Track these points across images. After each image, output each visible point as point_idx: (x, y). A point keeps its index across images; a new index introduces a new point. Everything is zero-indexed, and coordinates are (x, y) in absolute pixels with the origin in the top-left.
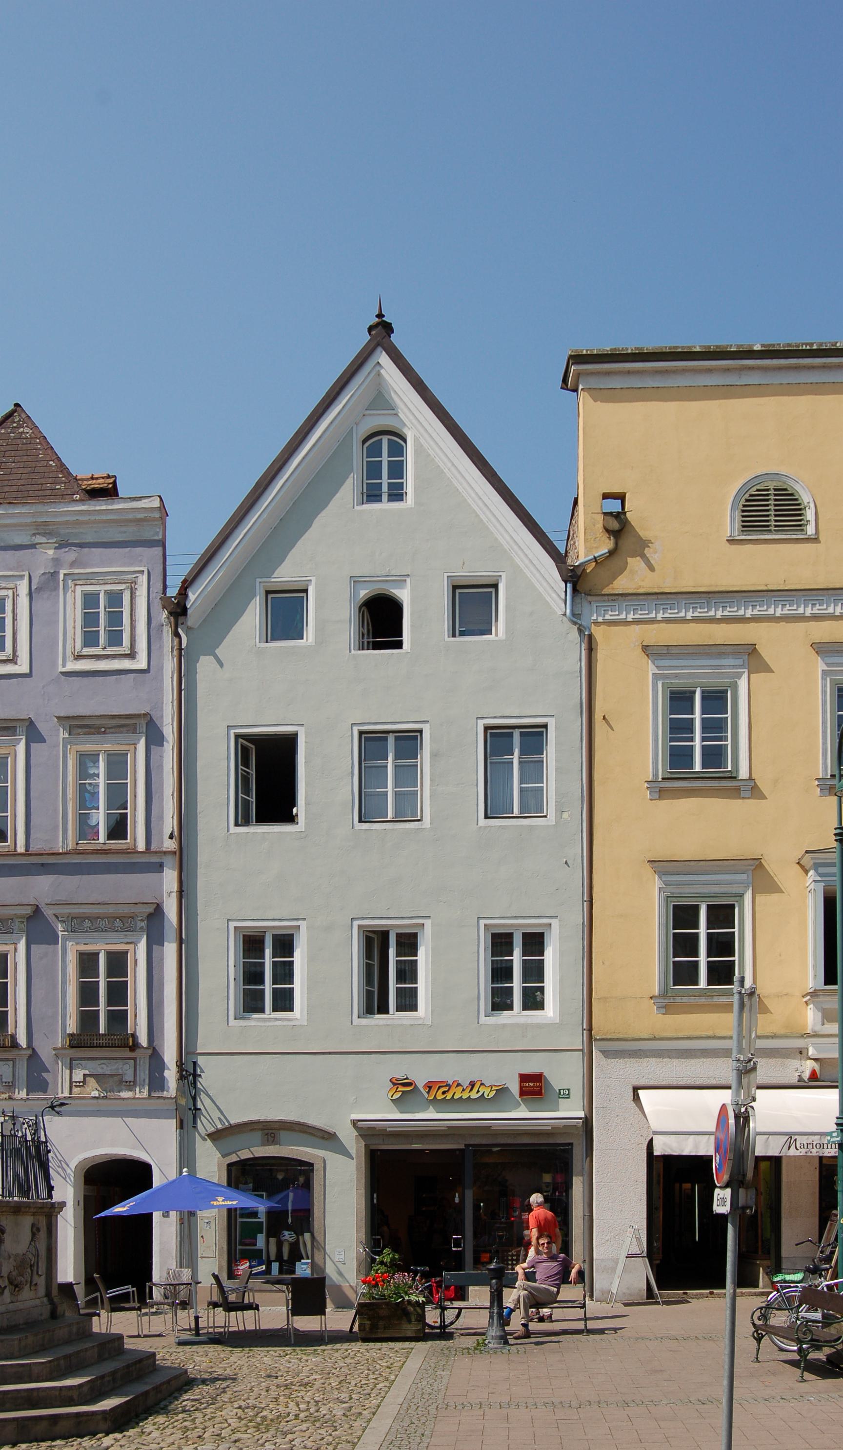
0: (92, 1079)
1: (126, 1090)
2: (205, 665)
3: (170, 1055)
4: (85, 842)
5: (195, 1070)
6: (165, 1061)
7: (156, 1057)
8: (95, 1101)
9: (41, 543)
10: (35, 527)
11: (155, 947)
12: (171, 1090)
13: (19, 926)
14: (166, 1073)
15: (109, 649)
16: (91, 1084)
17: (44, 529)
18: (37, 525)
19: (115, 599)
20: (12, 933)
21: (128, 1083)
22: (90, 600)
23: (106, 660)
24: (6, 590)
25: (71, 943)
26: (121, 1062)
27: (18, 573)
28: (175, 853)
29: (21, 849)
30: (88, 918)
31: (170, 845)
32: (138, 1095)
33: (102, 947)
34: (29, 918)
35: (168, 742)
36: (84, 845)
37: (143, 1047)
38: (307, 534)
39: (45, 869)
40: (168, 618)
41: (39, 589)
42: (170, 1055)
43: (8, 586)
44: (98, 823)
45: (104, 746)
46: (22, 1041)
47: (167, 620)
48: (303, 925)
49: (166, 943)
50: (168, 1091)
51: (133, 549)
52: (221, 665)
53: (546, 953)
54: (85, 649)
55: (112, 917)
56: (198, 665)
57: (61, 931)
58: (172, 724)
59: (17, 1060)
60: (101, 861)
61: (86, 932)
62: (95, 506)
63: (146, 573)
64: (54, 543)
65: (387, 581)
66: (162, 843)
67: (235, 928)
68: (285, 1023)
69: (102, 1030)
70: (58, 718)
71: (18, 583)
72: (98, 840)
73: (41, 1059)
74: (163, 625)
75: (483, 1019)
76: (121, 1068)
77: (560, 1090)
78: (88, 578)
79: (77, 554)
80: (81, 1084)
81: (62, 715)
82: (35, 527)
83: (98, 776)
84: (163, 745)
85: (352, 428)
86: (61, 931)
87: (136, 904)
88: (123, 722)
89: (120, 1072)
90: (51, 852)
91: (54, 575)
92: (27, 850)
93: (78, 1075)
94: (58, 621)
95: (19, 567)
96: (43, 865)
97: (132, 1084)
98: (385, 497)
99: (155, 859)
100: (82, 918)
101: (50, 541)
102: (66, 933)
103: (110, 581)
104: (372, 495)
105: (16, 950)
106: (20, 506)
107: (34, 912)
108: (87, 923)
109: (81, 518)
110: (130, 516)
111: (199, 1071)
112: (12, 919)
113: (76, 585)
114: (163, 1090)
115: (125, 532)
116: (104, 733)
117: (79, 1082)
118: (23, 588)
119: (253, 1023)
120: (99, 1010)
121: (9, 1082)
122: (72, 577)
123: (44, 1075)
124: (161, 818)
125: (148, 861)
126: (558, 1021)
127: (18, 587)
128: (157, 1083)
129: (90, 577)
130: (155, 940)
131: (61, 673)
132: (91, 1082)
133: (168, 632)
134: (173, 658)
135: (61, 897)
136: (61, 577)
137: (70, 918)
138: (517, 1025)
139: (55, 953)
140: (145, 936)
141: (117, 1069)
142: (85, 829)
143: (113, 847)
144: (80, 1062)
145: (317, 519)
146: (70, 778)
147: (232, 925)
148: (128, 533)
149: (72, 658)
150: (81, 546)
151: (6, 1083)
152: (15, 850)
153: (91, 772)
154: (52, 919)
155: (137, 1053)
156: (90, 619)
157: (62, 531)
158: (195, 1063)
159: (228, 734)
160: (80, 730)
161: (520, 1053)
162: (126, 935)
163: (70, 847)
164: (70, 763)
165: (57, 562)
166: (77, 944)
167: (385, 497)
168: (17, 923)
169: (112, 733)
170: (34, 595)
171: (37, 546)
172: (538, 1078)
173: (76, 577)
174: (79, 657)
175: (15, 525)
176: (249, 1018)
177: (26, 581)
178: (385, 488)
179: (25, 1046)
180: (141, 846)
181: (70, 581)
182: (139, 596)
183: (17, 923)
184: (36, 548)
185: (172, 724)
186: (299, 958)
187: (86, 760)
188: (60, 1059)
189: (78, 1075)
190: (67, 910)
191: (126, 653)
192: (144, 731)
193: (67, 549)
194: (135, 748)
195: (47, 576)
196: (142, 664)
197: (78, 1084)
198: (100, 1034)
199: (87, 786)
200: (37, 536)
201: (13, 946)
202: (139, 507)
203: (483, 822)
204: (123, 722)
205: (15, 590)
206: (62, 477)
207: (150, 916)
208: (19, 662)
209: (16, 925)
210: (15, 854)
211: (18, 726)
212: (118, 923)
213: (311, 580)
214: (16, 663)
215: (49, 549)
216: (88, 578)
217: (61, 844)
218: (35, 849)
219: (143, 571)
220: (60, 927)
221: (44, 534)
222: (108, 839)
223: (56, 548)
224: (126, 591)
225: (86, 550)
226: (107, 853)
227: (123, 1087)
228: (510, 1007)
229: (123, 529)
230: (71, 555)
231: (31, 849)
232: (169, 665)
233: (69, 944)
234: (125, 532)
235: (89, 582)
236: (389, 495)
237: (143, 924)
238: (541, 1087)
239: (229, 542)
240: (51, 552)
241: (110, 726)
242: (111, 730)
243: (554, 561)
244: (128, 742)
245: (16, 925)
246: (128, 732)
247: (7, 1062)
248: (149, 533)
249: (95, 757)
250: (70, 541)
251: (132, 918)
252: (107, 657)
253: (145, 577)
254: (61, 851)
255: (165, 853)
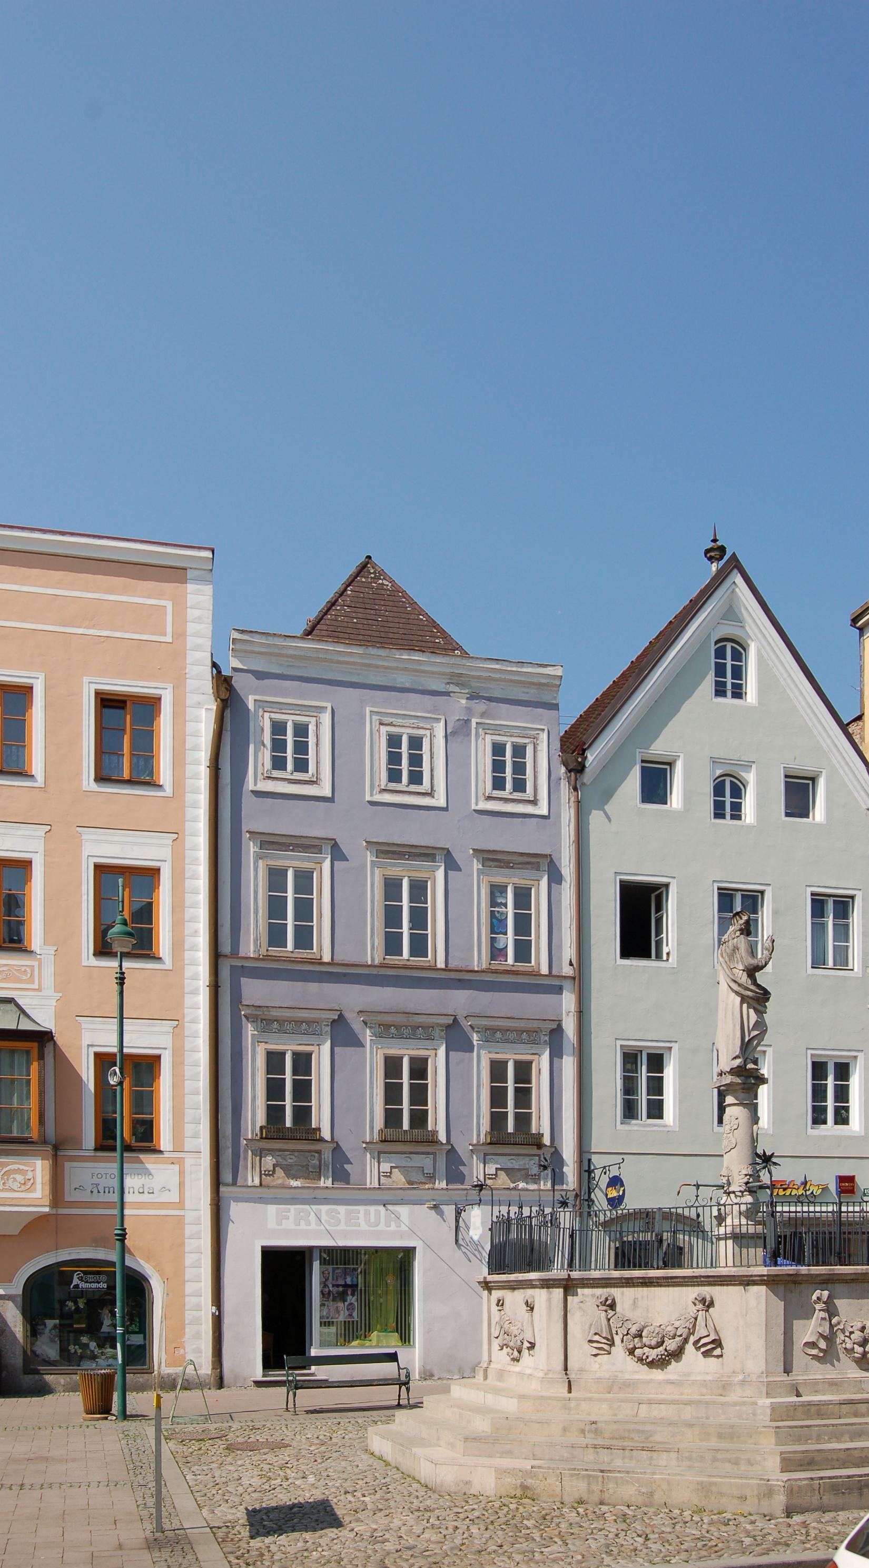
0: (503, 1172)
1: (532, 1182)
2: (595, 818)
3: (569, 1152)
4: (496, 962)
5: (589, 1167)
6: (564, 1157)
7: (557, 1155)
8: (508, 1192)
9: (454, 692)
10: (449, 677)
11: (555, 1059)
12: (569, 1184)
13: (439, 1034)
14: (565, 1169)
15: (515, 794)
16: (502, 1177)
17: (458, 679)
18: (453, 675)
19: (519, 751)
20: (433, 1039)
21: (534, 1177)
22: (498, 749)
23: (513, 803)
24: (424, 730)
25: (484, 1052)
26: (527, 1159)
27: (435, 717)
28: (574, 978)
29: (441, 964)
30: (499, 1030)
31: (568, 971)
32: (542, 1187)
33: (511, 1056)
34: (448, 1027)
35: (566, 881)
36: (496, 965)
37: (546, 1146)
38: (676, 717)
39: (461, 984)
40: (566, 774)
41: (453, 733)
42: (569, 1152)
43: (425, 726)
44: (507, 946)
45: (512, 880)
46: (442, 1137)
47: (565, 775)
48: (675, 1047)
49: (564, 1057)
50: (567, 1185)
51: (534, 709)
52: (610, 820)
53: (851, 1080)
54: (494, 792)
55: (519, 1031)
56: (590, 817)
57: (477, 1040)
58: (569, 866)
59: (437, 1154)
60: (510, 980)
61: (497, 1042)
62: (507, 666)
63: (546, 731)
64: (467, 693)
65: (736, 764)
66: (562, 969)
67: (621, 1046)
68: (661, 1129)
69: (510, 1129)
70: (474, 850)
71: (435, 725)
72: (506, 961)
73: (458, 1154)
74: (561, 779)
75: (810, 1131)
76: (528, 1163)
77: (864, 1189)
78: (497, 730)
79: (486, 707)
80: (494, 1177)
81: (476, 848)
82: (449, 677)
83: (505, 905)
84: (561, 884)
85: (710, 633)
86: (477, 1040)
87: (545, 1020)
88: (529, 860)
89: (527, 1166)
90: (467, 969)
91: (467, 722)
92: (446, 966)
93: (491, 1169)
94: (471, 764)
95: (435, 710)
96: (459, 980)
97: (537, 1177)
98: (729, 694)
99: (555, 982)
100: (494, 1030)
101: (462, 691)
102: (481, 1042)
103: (515, 734)
104: (720, 691)
105: (436, 1054)
106: (441, 656)
107: (453, 1021)
108: (498, 1035)
109: (493, 675)
110: (535, 680)
111: (592, 1167)
112: (433, 1027)
113: (486, 733)
114: (563, 1184)
115: (527, 693)
116: (512, 867)
117: (492, 1175)
118: (439, 730)
119: (636, 1128)
120: (507, 1112)
121: (430, 1174)
122: (482, 725)
123: (462, 1168)
124: (560, 947)
125: (549, 983)
126: (863, 1135)
127: (435, 729)
128: (558, 1178)
129: (498, 728)
130: (556, 1053)
131: (474, 810)
132: (502, 1174)
133: (564, 787)
134: (569, 807)
135: (476, 1010)
136: (474, 725)
137: (484, 1029)
138: (835, 1136)
139: (471, 1059)
140: (548, 1049)
141: (525, 1164)
142: (497, 953)
143: (521, 969)
144: (493, 1157)
145: (684, 705)
146: (483, 905)
147: (619, 1043)
148: (531, 694)
149: (483, 798)
150: (490, 699)
151: (427, 1174)
152: (436, 966)
153: (499, 901)
154: (468, 1029)
155: (543, 1150)
156: (498, 766)
157: (473, 684)
158: (590, 1160)
159: (615, 879)
160: (491, 863)
161: (837, 1159)
162: (532, 1047)
163: (484, 967)
164: (483, 892)
165: (469, 710)
166: (490, 1052)
167: (729, 694)
168: (437, 1031)
169: (519, 868)
170: (449, 738)
171: (451, 694)
172: (851, 1179)
173: (486, 727)
174: (489, 798)
175: (433, 673)
176: (629, 1124)
177: (443, 722)
178: (729, 686)
179: (444, 1142)
180: (544, 970)
181: (480, 730)
182: (540, 751)
183: (437, 1031)
184: (450, 696)
185: (569, 866)
186: (670, 1075)
187: (496, 891)
188: (476, 1153)
189: (491, 1169)
190: (484, 1022)
191: (531, 799)
192: (547, 869)
193: (477, 701)
194: (539, 884)
195: (461, 722)
196: (543, 810)
197: (491, 1176)
198: (508, 1133)
199: (496, 913)
200: (451, 685)
201: (434, 1052)
202: (545, 673)
203: (810, 971)
204: (529, 860)
205: (432, 731)
206: (437, 632)
207: (552, 1031)
208: (436, 795)
209: (437, 1032)
210: (435, 969)
211: (437, 854)
212: (524, 1036)
213: (679, 756)
214: (433, 797)
215: (462, 699)
216: (497, 730)
217: (476, 963)
218: (453, 966)
219: (544, 730)
220: (475, 1037)
221: (457, 685)
222: (515, 962)
223: (467, 699)
224: (529, 745)
225: (494, 703)
226: (517, 974)
227: (530, 1180)
228: (825, 1122)
229: (526, 690)
230: (481, 706)
231: (449, 965)
232: (567, 815)
233: (483, 1052)
234: (527, 693)
235: (497, 732)
236: (733, 693)
237: (547, 1038)
238: (854, 1187)
239: (619, 715)
240: (464, 701)
241: (517, 862)
242: (518, 866)
243: (866, 766)
244: (533, 878)
245: (437, 1032)
246: (532, 869)
247: (428, 1156)
248: (547, 698)
249: (502, 889)
250: (480, 694)
251: (537, 1032)
252: (513, 801)
253: (545, 735)
254: (476, 969)
255: (565, 977)
